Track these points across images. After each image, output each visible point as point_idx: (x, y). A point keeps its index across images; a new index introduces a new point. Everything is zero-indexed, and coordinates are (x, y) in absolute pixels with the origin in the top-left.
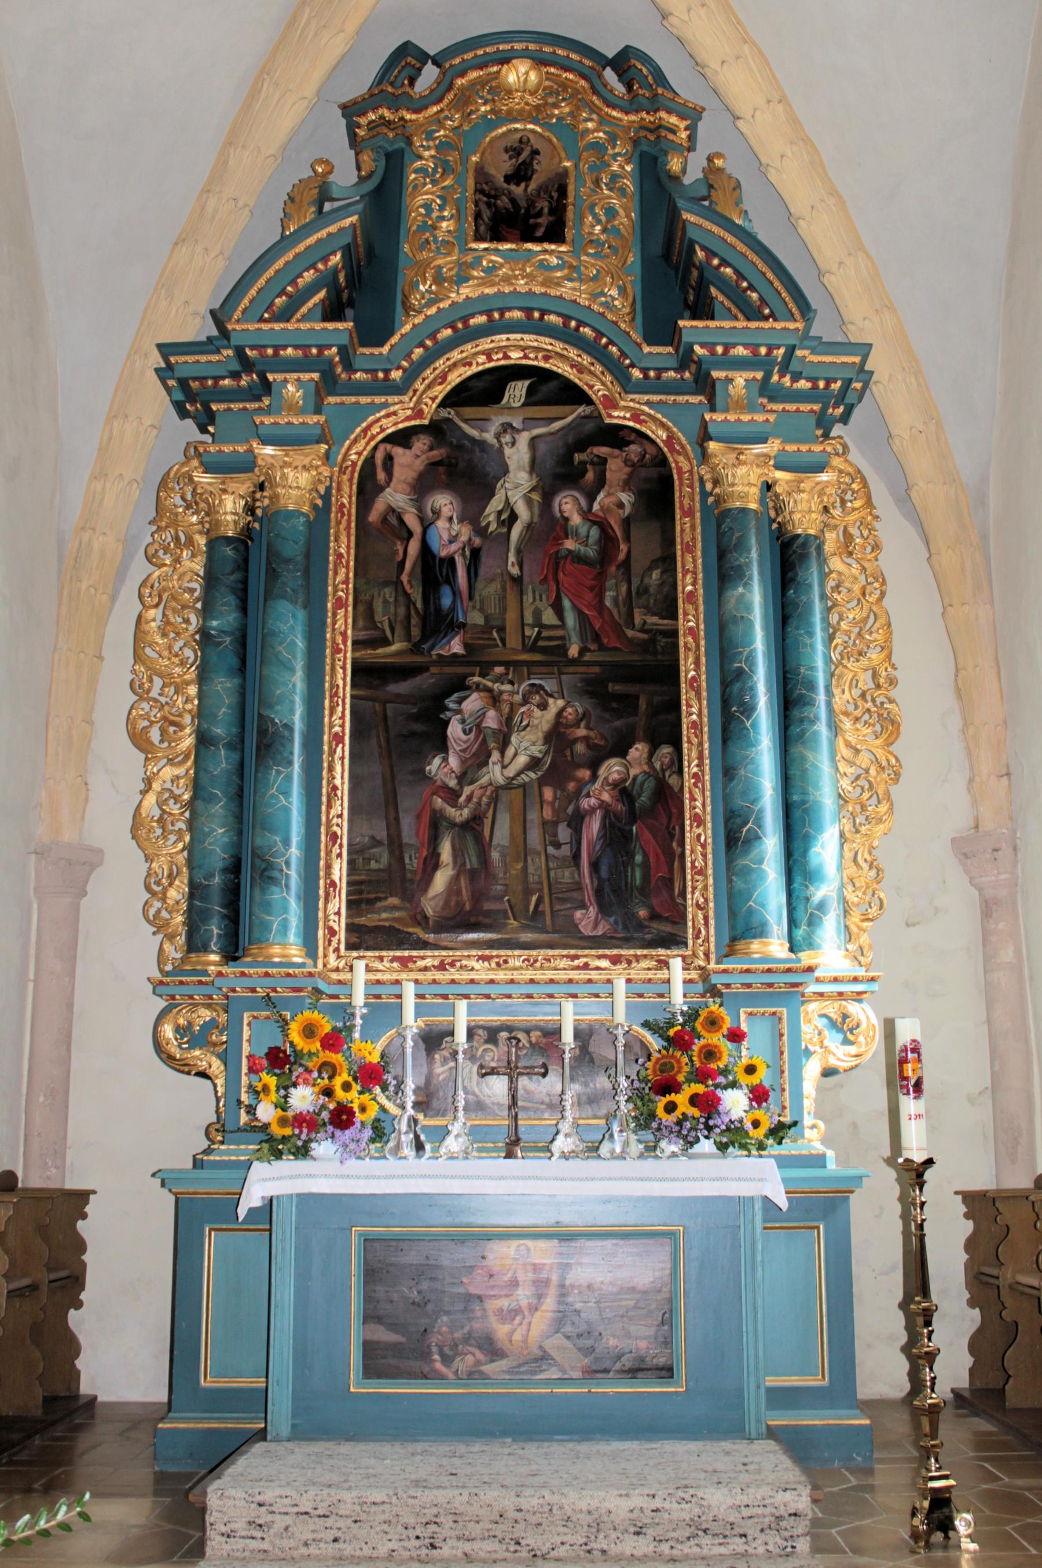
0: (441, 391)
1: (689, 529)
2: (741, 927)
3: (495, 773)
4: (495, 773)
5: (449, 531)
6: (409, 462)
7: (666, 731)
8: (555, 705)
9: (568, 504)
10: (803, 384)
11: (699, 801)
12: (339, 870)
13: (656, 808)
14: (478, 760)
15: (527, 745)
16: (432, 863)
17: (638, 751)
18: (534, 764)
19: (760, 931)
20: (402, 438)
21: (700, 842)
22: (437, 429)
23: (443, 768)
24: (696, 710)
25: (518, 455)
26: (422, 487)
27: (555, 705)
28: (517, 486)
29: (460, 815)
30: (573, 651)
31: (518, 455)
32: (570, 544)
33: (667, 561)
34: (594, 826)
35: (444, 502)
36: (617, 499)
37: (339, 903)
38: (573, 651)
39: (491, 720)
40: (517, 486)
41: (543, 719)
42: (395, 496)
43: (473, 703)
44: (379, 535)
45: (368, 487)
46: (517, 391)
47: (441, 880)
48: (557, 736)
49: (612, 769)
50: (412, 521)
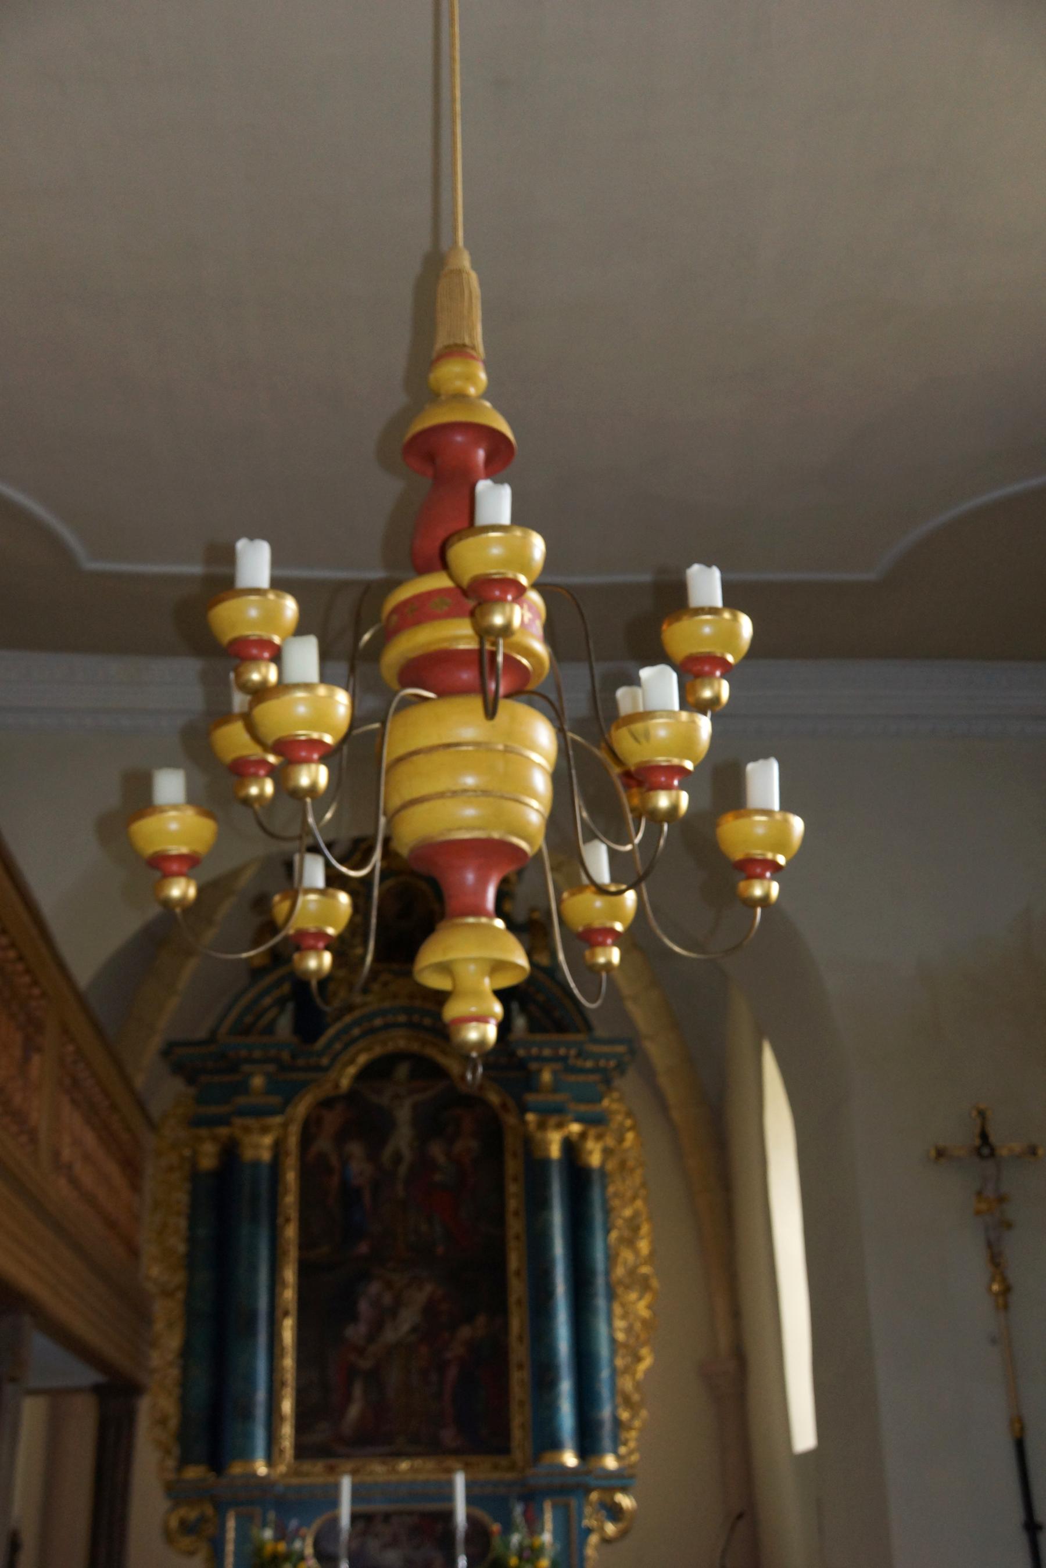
0: (352, 1070)
1: (513, 1166)
2: (548, 1441)
3: (390, 1335)
4: (390, 1335)
5: (359, 1167)
6: (332, 1120)
7: (500, 1308)
8: (428, 1288)
9: (436, 1150)
10: (589, 1064)
11: (519, 1352)
12: (287, 1406)
13: (491, 1359)
14: (377, 1327)
15: (408, 1319)
16: (348, 1399)
17: (481, 1320)
18: (414, 1329)
19: (556, 1445)
20: (327, 1103)
21: (519, 1381)
22: (352, 1097)
23: (356, 1332)
24: (517, 1288)
25: (404, 1114)
26: (341, 1137)
27: (428, 1288)
28: (402, 1137)
29: (365, 1364)
30: (440, 1250)
31: (404, 1114)
32: (438, 1177)
33: (500, 1189)
34: (453, 1372)
35: (355, 1148)
36: (467, 1145)
37: (287, 1430)
38: (440, 1250)
39: (387, 1299)
40: (402, 1137)
41: (420, 1296)
42: (323, 1144)
43: (374, 1288)
44: (312, 1171)
45: (306, 1139)
46: (402, 1071)
47: (354, 1411)
48: (430, 1309)
49: (465, 1332)
50: (334, 1161)
